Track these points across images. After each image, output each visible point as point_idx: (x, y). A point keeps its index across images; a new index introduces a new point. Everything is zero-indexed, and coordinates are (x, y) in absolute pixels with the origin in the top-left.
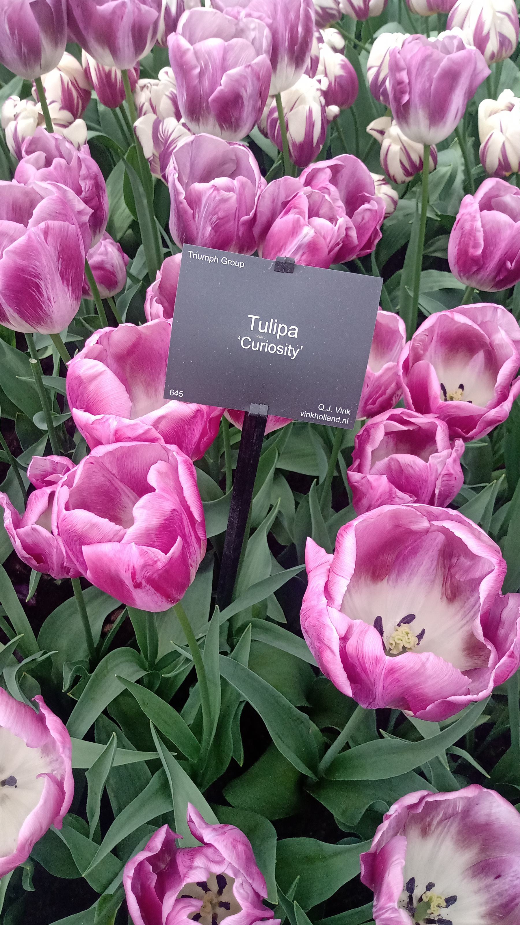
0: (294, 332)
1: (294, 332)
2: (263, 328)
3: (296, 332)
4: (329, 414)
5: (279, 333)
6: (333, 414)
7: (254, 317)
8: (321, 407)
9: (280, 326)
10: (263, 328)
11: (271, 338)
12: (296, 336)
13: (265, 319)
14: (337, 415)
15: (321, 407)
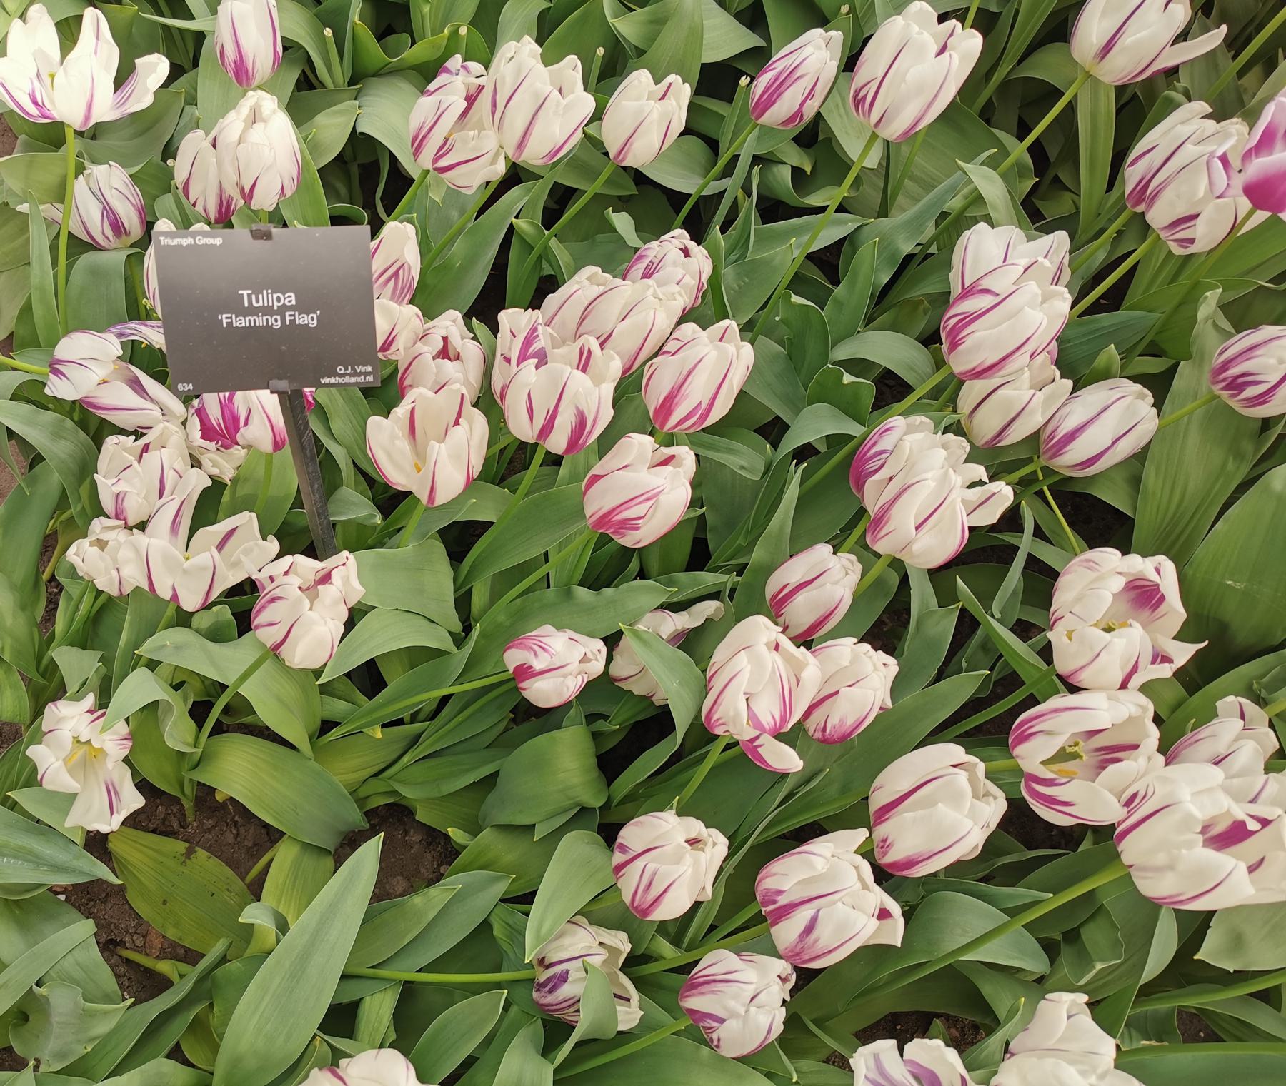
0: (291, 299)
1: (291, 299)
2: (258, 301)
3: (293, 298)
4: (350, 375)
5: (276, 304)
6: (355, 374)
7: (245, 293)
8: (340, 370)
9: (275, 296)
10: (258, 301)
11: (268, 310)
12: (294, 303)
13: (257, 292)
14: (360, 374)
15: (340, 370)
